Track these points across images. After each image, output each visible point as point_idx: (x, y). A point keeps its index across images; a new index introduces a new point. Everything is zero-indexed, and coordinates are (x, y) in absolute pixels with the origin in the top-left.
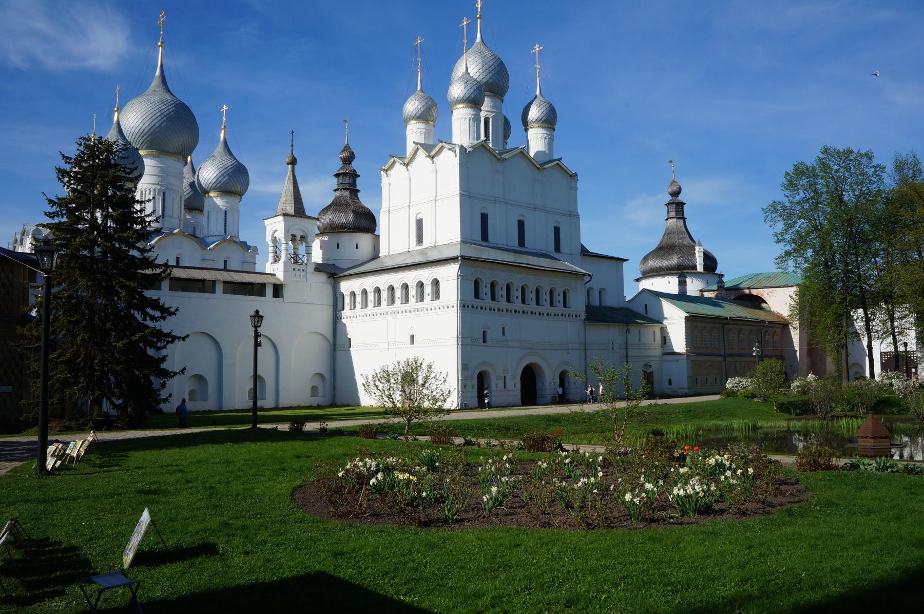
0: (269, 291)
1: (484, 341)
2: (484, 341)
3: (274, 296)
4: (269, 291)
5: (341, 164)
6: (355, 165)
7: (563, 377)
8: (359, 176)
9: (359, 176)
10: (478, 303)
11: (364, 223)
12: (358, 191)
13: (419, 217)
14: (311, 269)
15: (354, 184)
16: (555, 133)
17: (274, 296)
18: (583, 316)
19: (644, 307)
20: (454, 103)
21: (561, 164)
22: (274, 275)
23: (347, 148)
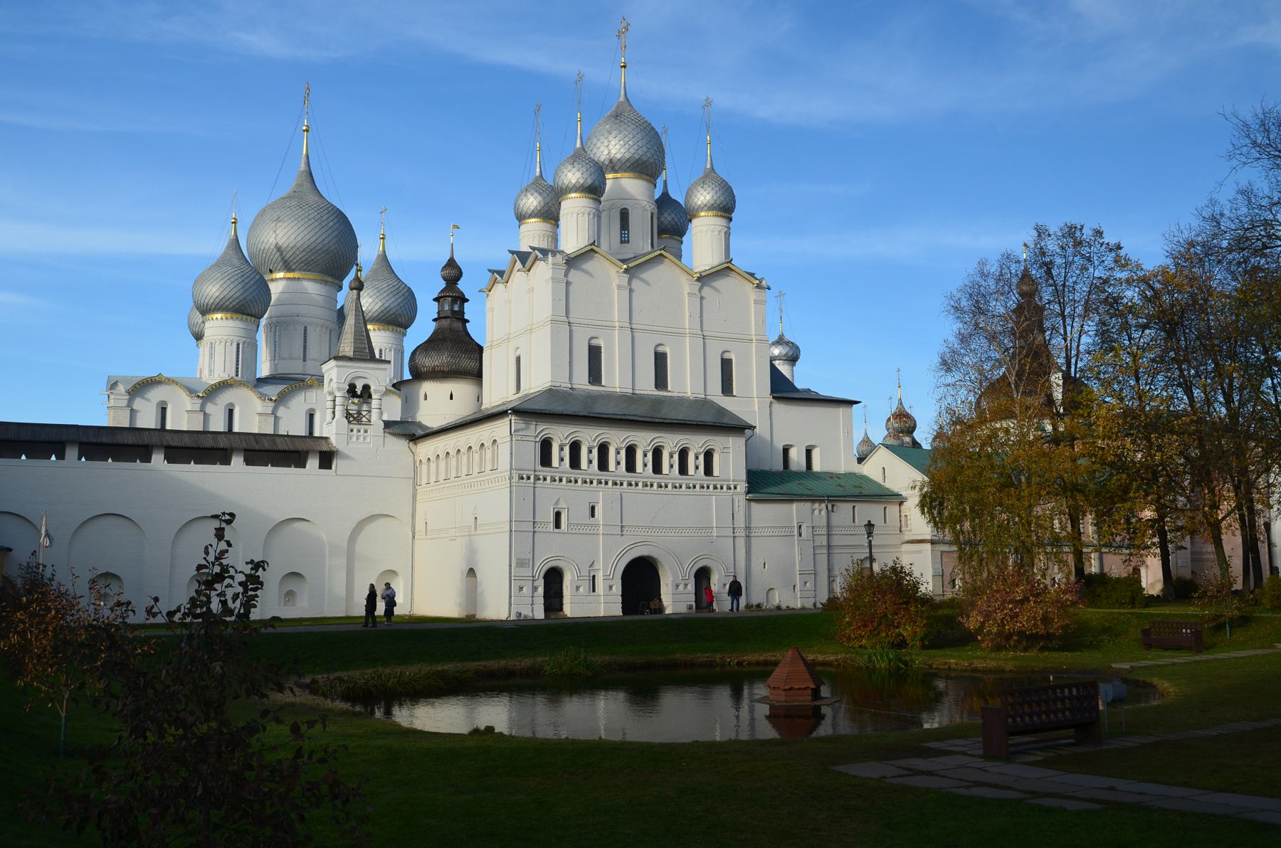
0: (313, 463)
1: (558, 525)
2: (558, 525)
4: (313, 463)
6: (462, 285)
8: (467, 300)
9: (467, 300)
11: (467, 363)
12: (468, 321)
16: (731, 224)
17: (320, 468)
18: (742, 487)
19: (881, 471)
20: (563, 191)
21: (732, 267)
23: (451, 263)
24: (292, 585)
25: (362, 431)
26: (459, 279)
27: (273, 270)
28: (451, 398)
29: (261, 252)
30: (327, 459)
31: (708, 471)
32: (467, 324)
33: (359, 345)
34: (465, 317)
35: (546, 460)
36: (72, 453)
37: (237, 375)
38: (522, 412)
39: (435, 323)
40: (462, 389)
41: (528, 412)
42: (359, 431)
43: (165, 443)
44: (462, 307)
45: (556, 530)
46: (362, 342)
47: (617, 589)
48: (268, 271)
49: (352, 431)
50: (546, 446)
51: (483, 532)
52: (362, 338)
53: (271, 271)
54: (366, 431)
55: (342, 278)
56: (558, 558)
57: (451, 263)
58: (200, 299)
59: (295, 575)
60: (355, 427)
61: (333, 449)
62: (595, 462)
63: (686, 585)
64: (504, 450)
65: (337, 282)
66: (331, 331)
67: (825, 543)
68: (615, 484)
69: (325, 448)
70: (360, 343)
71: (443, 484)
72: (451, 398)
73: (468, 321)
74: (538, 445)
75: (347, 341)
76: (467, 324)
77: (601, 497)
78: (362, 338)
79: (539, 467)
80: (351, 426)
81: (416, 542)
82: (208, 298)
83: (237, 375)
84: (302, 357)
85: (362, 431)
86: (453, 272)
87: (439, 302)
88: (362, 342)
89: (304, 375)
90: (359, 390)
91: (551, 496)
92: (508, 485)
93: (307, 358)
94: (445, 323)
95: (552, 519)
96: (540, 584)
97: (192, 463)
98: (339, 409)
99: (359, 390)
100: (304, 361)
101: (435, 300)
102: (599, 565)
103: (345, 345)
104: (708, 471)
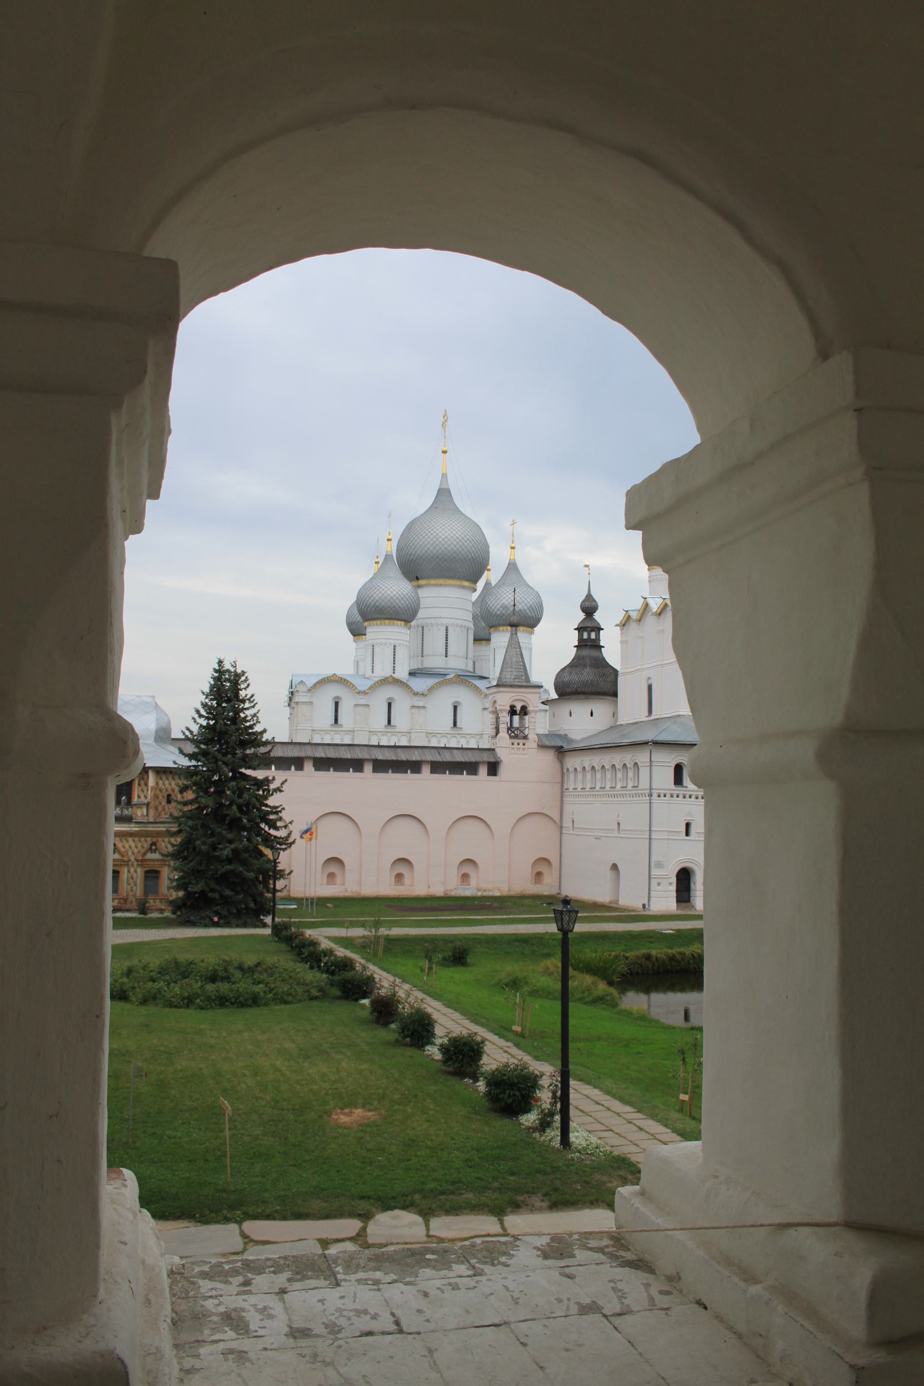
0: (483, 770)
1: (687, 834)
2: (687, 834)
3: (489, 774)
4: (483, 770)
5: (582, 616)
6: (597, 616)
8: (602, 629)
9: (602, 629)
10: (679, 790)
12: (603, 647)
13: (650, 682)
14: (532, 742)
15: (598, 639)
17: (489, 774)
22: (493, 750)
23: (589, 597)
24: (467, 869)
25: (521, 744)
26: (595, 611)
27: (419, 577)
28: (592, 715)
29: (409, 563)
30: (493, 768)
32: (602, 649)
33: (517, 673)
34: (601, 644)
36: (309, 766)
37: (394, 673)
38: (660, 743)
39: (576, 649)
40: (601, 708)
41: (664, 743)
42: (518, 744)
43: (373, 757)
44: (598, 635)
45: (687, 838)
46: (520, 670)
48: (415, 578)
49: (513, 744)
50: (678, 769)
51: (622, 836)
52: (519, 667)
53: (417, 578)
54: (524, 744)
55: (475, 581)
57: (589, 597)
58: (363, 608)
59: (470, 861)
60: (516, 741)
61: (499, 760)
65: (472, 585)
66: (468, 629)
69: (492, 760)
70: (519, 671)
71: (588, 791)
72: (592, 715)
73: (603, 647)
75: (507, 670)
76: (602, 649)
78: (519, 667)
79: (672, 786)
80: (513, 741)
81: (564, 836)
82: (371, 607)
83: (394, 673)
84: (444, 653)
85: (521, 744)
86: (589, 608)
87: (579, 632)
88: (520, 670)
89: (446, 669)
90: (518, 708)
92: (648, 801)
93: (448, 654)
94: (586, 652)
96: (674, 880)
97: (390, 771)
98: (503, 728)
99: (518, 708)
100: (446, 656)
101: (575, 629)
103: (507, 673)
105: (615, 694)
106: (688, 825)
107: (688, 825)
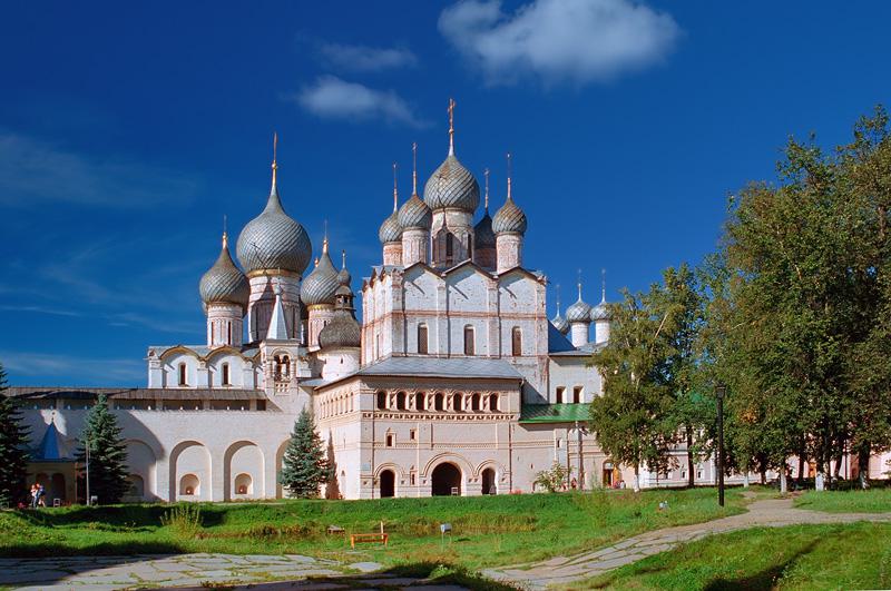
1: (389, 444)
7: (488, 475)
30: (262, 405)
31: (493, 407)
35: (381, 405)
47: (429, 483)
56: (389, 464)
62: (433, 405)
63: (476, 480)
64: (357, 397)
67: (577, 451)
68: (427, 417)
74: (376, 397)
77: (420, 426)
91: (382, 427)
95: (385, 440)
102: (417, 468)
104: (493, 407)
105: (360, 346)
106: (389, 439)
107: (389, 439)
